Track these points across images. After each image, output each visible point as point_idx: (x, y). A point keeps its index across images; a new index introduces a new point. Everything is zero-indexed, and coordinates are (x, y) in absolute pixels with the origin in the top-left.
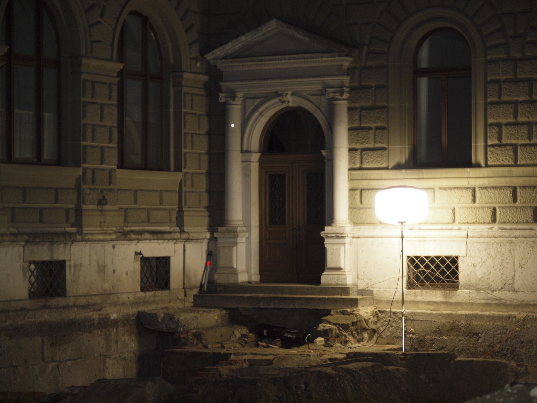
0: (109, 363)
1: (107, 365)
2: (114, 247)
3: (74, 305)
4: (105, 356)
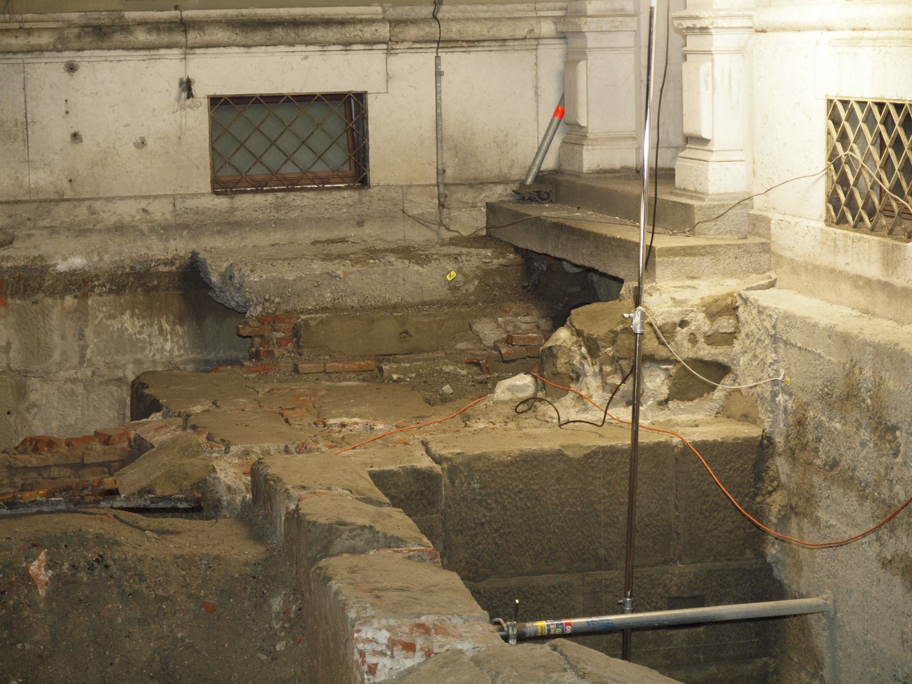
0: (38, 391)
1: (33, 397)
2: (71, 68)
4: (25, 373)
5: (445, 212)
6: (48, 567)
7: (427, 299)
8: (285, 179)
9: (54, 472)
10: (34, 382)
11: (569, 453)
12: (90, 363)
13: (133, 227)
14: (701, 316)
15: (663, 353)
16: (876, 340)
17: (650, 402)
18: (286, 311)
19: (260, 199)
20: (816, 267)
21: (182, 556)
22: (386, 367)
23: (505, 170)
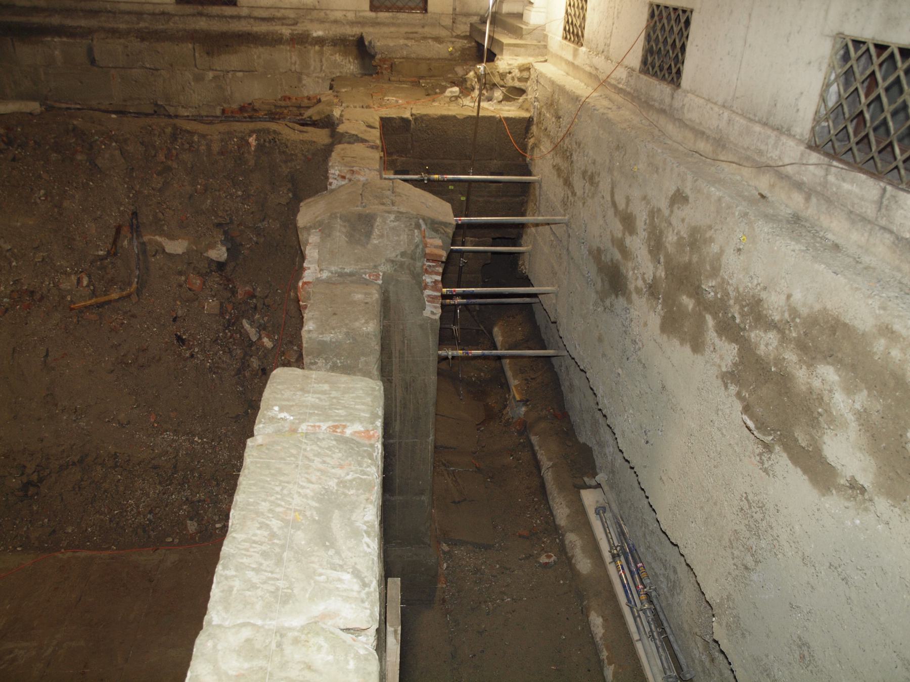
0: (306, 80)
1: (304, 82)
3: (249, 17)
5: (455, 25)
6: (256, 140)
7: (441, 57)
8: (398, 7)
9: (291, 109)
10: (304, 77)
11: (458, 117)
12: (324, 72)
13: (342, 22)
14: (517, 71)
15: (502, 83)
16: (560, 84)
17: (495, 101)
18: (390, 58)
19: (387, 14)
20: (557, 55)
21: (303, 141)
22: (421, 81)
23: (478, 10)
